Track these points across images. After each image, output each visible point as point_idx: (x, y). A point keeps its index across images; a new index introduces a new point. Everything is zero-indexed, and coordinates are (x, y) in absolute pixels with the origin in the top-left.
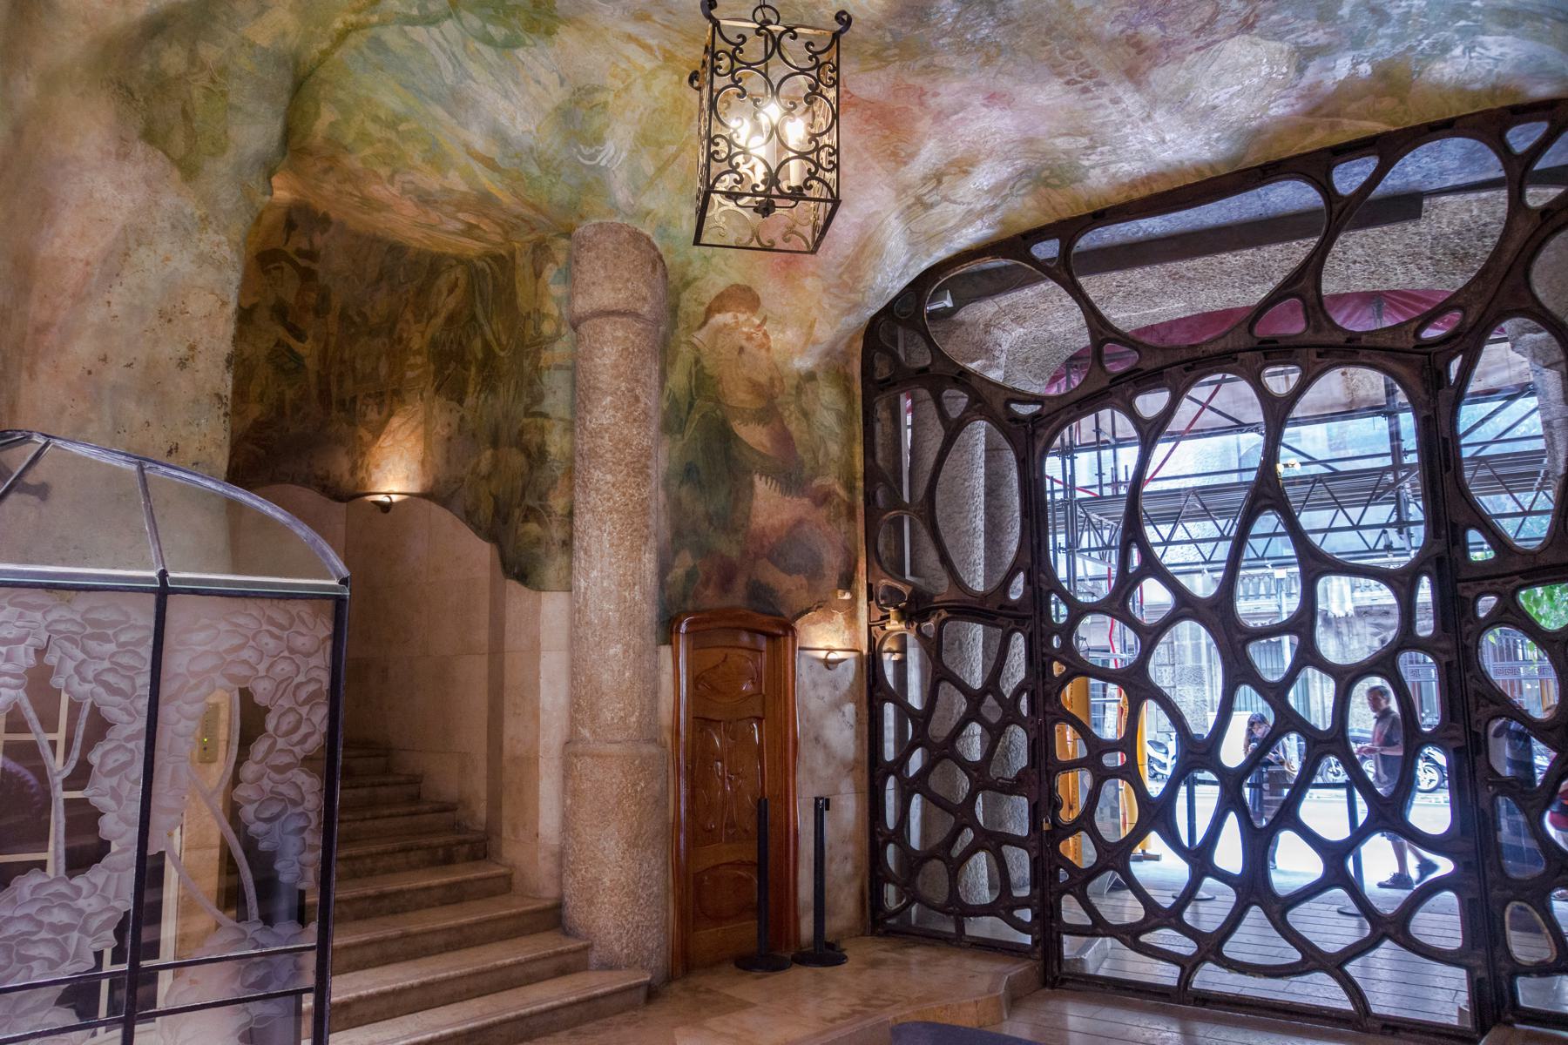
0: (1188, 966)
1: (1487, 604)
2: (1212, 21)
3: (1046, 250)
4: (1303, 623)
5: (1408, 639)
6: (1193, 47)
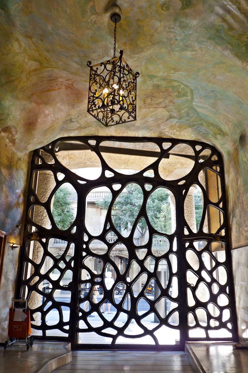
0: (114, 337)
1: (187, 244)
2: (160, 103)
3: (93, 142)
4: (149, 246)
5: (171, 251)
6: (153, 107)
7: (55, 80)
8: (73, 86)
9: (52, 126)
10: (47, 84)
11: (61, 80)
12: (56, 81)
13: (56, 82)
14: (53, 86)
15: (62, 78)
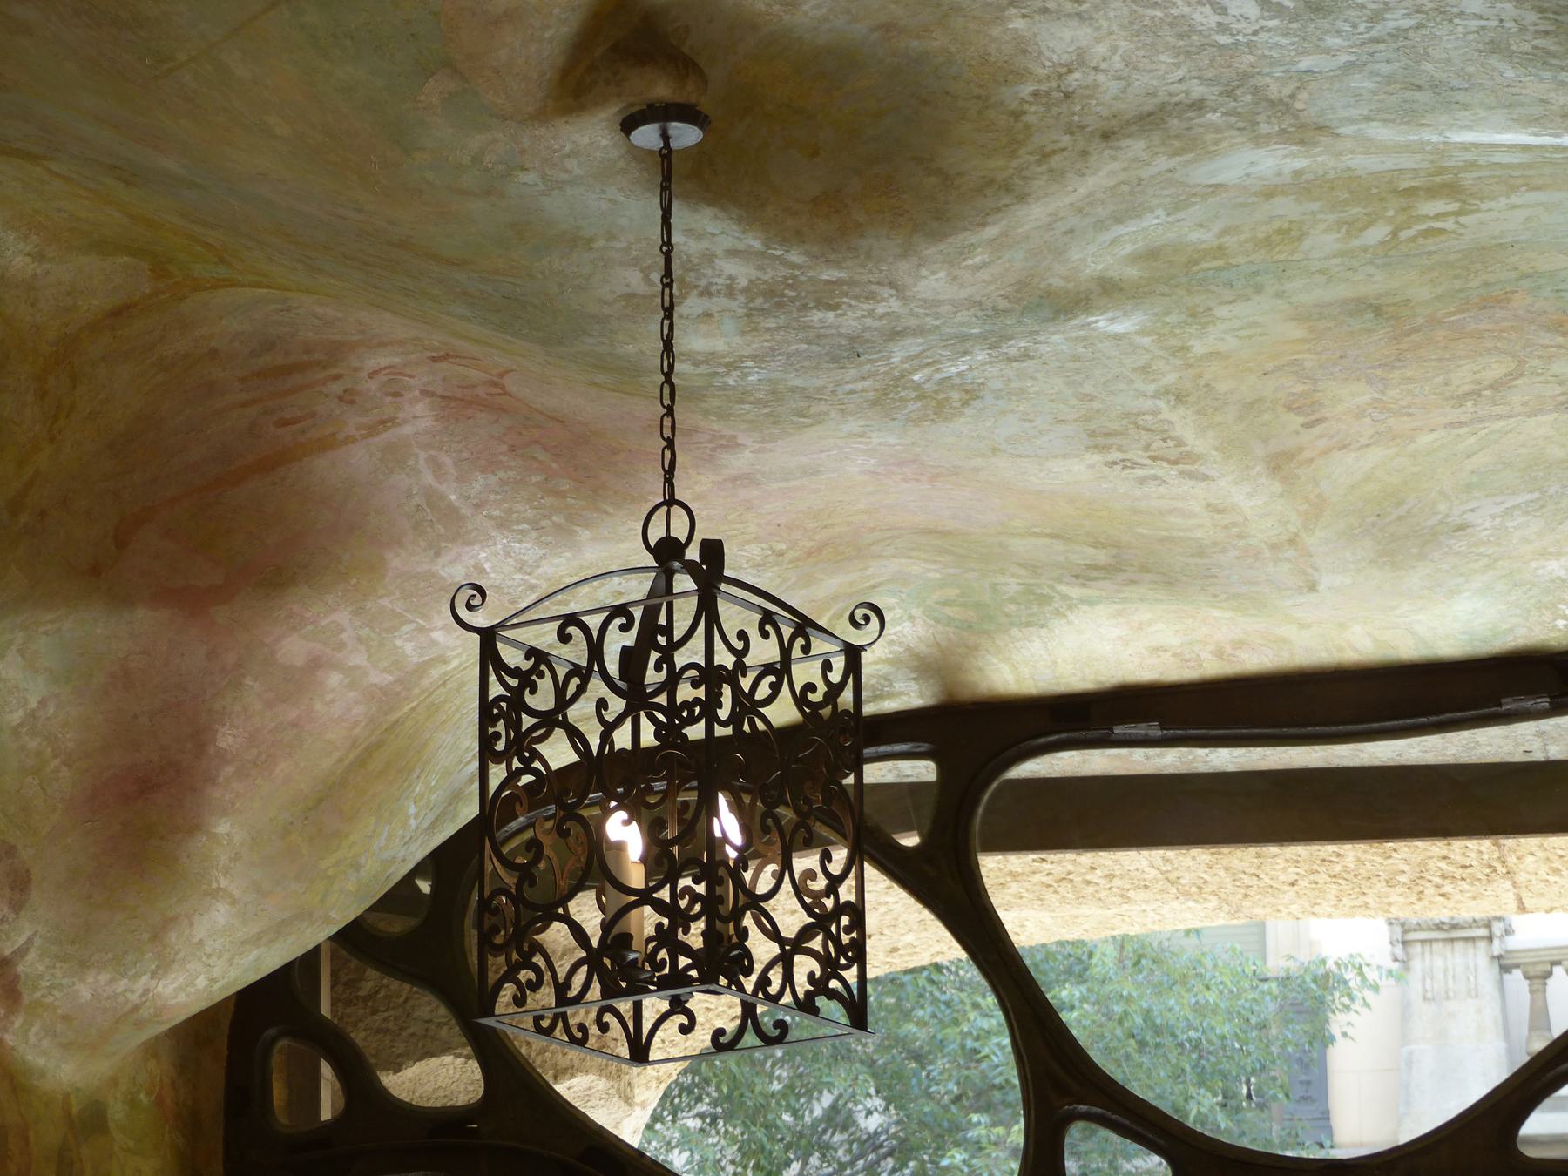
7: (324, 368)
8: (506, 393)
9: (379, 745)
10: (244, 405)
11: (381, 360)
12: (333, 371)
13: (336, 378)
14: (314, 415)
15: (382, 344)
